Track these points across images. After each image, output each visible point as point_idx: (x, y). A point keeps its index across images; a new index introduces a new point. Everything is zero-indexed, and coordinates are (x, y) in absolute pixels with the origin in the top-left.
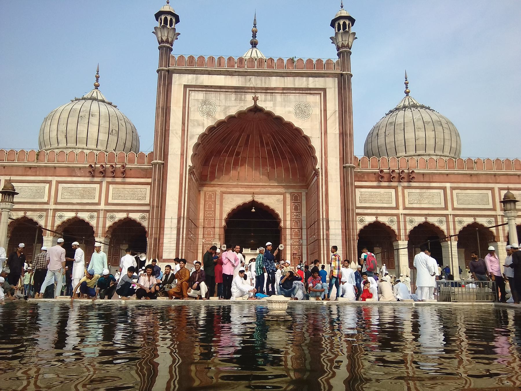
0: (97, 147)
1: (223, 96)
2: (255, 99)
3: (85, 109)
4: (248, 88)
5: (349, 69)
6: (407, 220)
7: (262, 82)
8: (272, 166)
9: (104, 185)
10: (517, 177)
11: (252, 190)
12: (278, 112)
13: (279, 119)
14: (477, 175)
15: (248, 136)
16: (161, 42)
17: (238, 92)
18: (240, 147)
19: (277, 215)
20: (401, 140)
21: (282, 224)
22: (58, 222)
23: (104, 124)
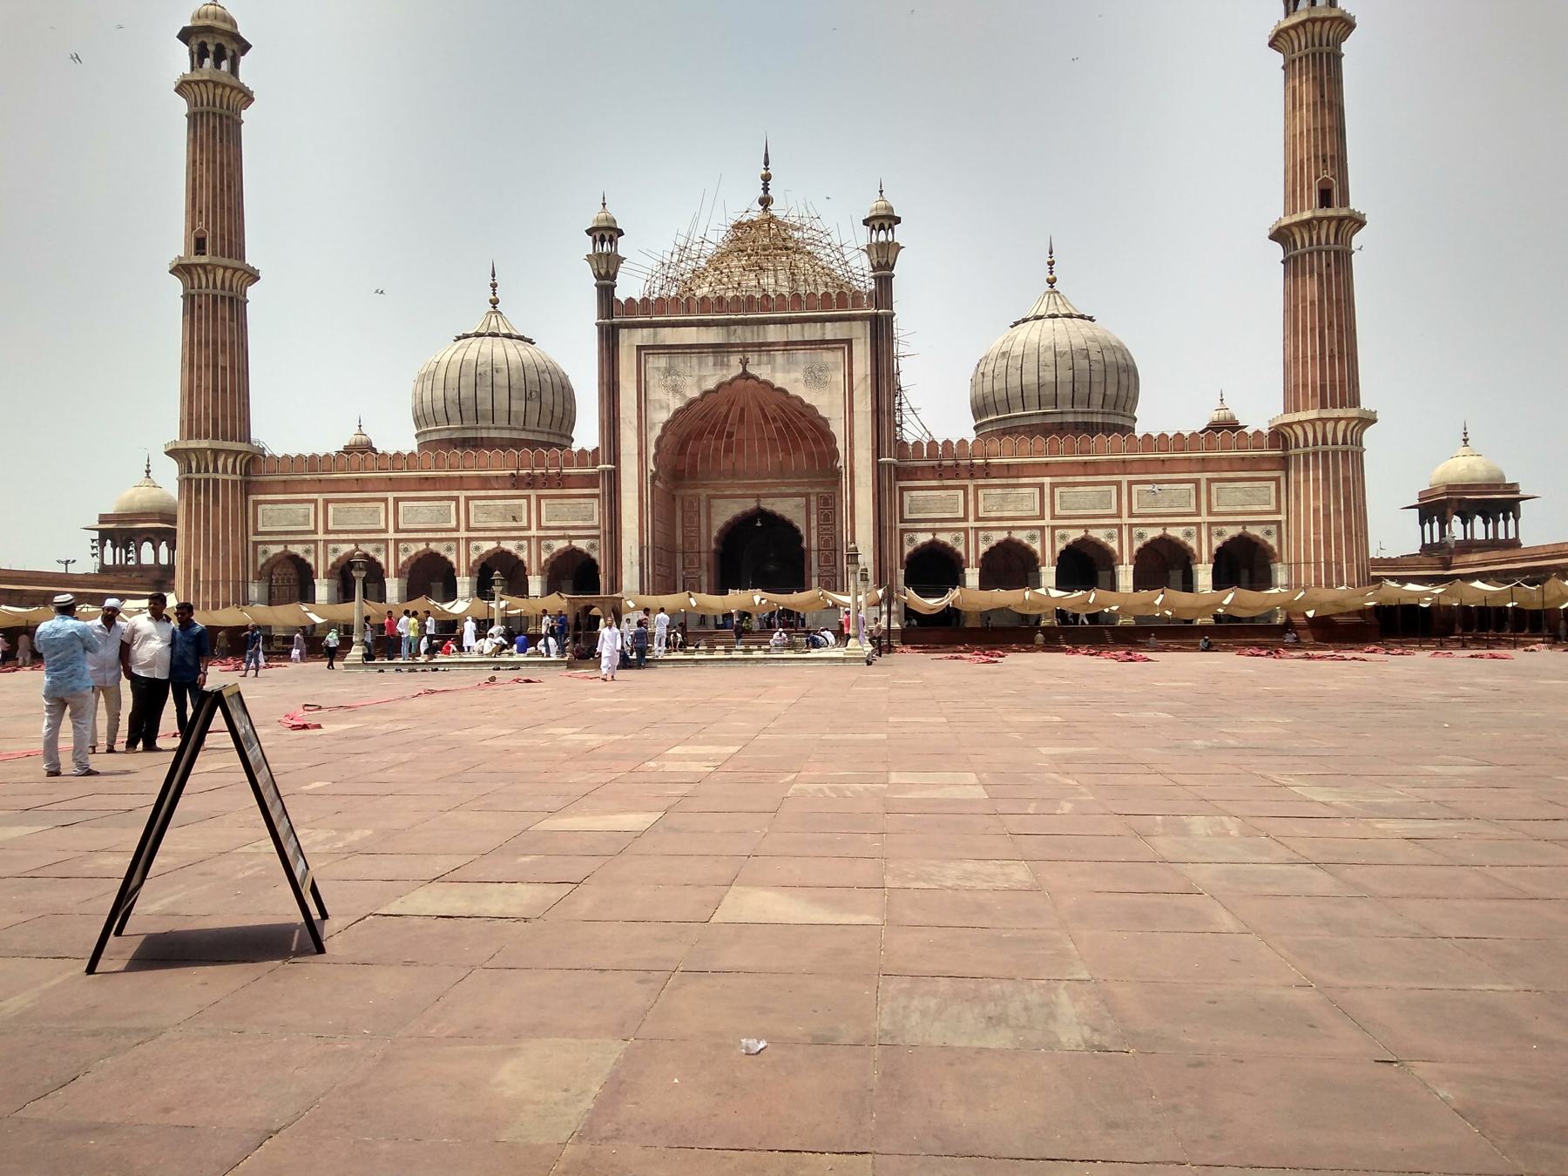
0: (509, 423)
1: (695, 360)
2: (745, 363)
3: (483, 360)
4: (732, 345)
5: (890, 306)
10: (1161, 463)
12: (779, 380)
13: (782, 391)
14: (1094, 463)
15: (743, 410)
16: (598, 276)
17: (717, 352)
18: (731, 425)
19: (797, 531)
20: (1015, 387)
21: (805, 545)
22: (474, 556)
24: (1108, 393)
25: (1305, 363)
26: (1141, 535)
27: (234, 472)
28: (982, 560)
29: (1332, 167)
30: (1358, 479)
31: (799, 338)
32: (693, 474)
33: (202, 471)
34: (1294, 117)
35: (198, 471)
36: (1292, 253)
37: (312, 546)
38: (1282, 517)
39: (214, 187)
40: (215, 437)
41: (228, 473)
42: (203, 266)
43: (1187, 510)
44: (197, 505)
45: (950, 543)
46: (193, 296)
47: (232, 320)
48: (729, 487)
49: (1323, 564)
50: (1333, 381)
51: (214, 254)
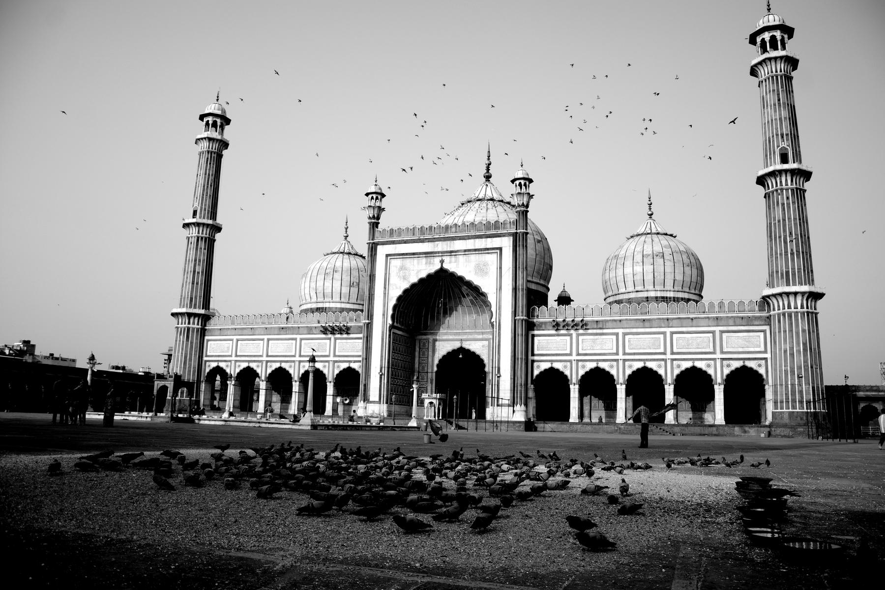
1: (416, 260)
2: (442, 262)
4: (436, 253)
6: (579, 365)
7: (447, 246)
8: (477, 313)
9: (333, 340)
10: (691, 320)
11: (460, 337)
12: (460, 272)
14: (649, 320)
17: (428, 257)
19: (482, 361)
20: (621, 276)
23: (346, 278)
24: (677, 278)
25: (776, 258)
26: (679, 366)
27: (198, 324)
28: (580, 380)
29: (787, 140)
30: (813, 331)
31: (472, 247)
32: (426, 328)
33: (183, 324)
34: (764, 113)
35: (182, 324)
36: (767, 191)
37: (230, 363)
38: (768, 356)
39: (204, 186)
40: (190, 307)
41: (196, 325)
42: (194, 224)
43: (707, 350)
44: (180, 341)
45: (561, 370)
46: (189, 238)
47: (205, 249)
48: (446, 334)
49: (790, 386)
50: (793, 269)
51: (200, 218)
